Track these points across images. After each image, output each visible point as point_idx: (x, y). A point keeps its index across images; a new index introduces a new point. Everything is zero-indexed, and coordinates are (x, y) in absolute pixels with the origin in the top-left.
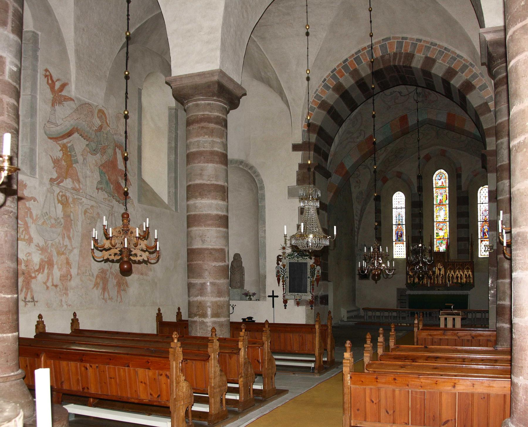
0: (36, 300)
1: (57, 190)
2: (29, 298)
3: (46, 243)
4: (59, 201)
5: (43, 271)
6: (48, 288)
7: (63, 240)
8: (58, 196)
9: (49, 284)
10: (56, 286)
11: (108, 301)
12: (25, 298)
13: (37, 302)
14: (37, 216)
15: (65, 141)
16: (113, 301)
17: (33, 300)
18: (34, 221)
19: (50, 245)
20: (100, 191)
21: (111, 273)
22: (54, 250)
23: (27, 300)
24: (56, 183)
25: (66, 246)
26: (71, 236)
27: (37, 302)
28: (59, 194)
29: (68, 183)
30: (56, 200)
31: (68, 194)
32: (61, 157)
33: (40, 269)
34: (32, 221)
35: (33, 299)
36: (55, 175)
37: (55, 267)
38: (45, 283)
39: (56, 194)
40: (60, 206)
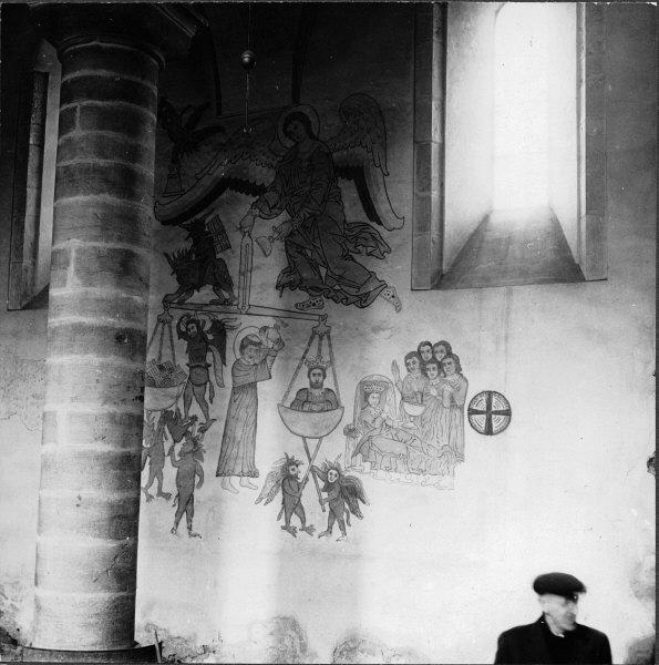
1: (177, 314)
4: (182, 335)
7: (187, 405)
10: (167, 496)
11: (299, 534)
15: (199, 216)
16: (316, 534)
19: (157, 419)
25: (195, 418)
26: (207, 396)
29: (204, 295)
30: (174, 331)
31: (201, 317)
37: (168, 459)
40: (182, 345)
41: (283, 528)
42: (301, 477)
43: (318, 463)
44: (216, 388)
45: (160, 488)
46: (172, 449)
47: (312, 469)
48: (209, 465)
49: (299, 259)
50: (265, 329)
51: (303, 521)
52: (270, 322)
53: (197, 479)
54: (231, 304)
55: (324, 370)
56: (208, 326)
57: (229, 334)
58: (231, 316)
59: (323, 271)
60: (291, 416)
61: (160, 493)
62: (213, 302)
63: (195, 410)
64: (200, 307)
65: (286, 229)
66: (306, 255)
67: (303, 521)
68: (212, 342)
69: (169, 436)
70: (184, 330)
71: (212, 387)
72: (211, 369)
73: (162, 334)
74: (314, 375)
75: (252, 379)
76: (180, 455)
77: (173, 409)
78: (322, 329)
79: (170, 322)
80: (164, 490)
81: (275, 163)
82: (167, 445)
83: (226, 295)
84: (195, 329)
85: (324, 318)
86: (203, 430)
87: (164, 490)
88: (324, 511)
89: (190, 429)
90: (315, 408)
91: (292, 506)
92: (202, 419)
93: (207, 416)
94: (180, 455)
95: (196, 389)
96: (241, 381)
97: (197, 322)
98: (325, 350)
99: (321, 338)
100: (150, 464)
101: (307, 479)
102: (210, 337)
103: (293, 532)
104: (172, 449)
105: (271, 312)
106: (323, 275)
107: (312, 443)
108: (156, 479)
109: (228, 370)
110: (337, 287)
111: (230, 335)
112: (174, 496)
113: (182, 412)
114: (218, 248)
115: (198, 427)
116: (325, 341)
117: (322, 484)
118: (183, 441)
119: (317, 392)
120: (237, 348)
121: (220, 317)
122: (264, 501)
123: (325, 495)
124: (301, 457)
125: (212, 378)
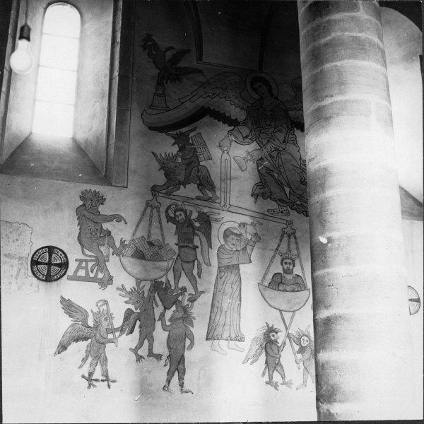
0: (111, 377)
1: (166, 202)
2: (98, 374)
3: (138, 284)
4: (170, 219)
5: (131, 332)
6: (139, 358)
7: (177, 278)
8: (167, 212)
9: (143, 351)
10: (159, 357)
11: (280, 387)
12: (91, 374)
13: (114, 381)
14: (122, 242)
15: (184, 130)
16: (294, 387)
17: (106, 379)
18: (118, 253)
20: (260, 198)
21: (288, 336)
22: (156, 295)
23: (94, 377)
24: (164, 192)
25: (184, 289)
26: (195, 272)
27: (114, 381)
28: (169, 207)
30: (163, 216)
31: (188, 208)
32: (175, 153)
33: (122, 326)
34: (111, 250)
35: (107, 377)
36: (161, 179)
37: (158, 324)
38: (135, 351)
39: (162, 209)
41: (267, 383)
42: (280, 341)
43: (293, 331)
44: (204, 266)
45: (150, 349)
46: (162, 316)
47: (288, 336)
48: (199, 330)
49: (269, 178)
50: (243, 225)
51: (283, 377)
52: (248, 220)
53: (188, 342)
54: (213, 202)
55: (293, 261)
56: (195, 216)
57: (213, 224)
58: (214, 210)
59: (287, 190)
60: (270, 293)
61: (151, 354)
62: (198, 198)
63: (184, 282)
64: (187, 199)
65: (257, 155)
66: (273, 176)
67: (283, 377)
68: (199, 229)
69: (160, 303)
70: (173, 216)
71: (199, 265)
72: (198, 250)
73: (151, 216)
74: (286, 263)
75: (235, 262)
76: (170, 320)
77: (164, 280)
78: (289, 230)
79: (158, 208)
80: (155, 351)
81: (245, 107)
82: (158, 311)
83: (210, 194)
84: (183, 216)
85: (290, 223)
86: (192, 300)
87: (155, 351)
88: (299, 369)
89: (180, 298)
90: (288, 288)
91: (273, 364)
92: (191, 290)
93: (196, 288)
94: (170, 320)
95: (186, 266)
96: (225, 262)
97: (185, 212)
98: (293, 246)
99: (289, 236)
100: (140, 327)
101: (284, 343)
102: (197, 224)
103: (276, 386)
104: (162, 316)
105: (247, 212)
106: (287, 192)
107: (287, 316)
108: (146, 341)
109: (214, 252)
110: (298, 202)
111: (215, 226)
112: (164, 358)
113: (172, 283)
114: (201, 158)
115: (187, 297)
116: (292, 240)
117: (297, 348)
118: (174, 308)
119: (289, 277)
120: (221, 236)
121: (205, 210)
122: (250, 361)
123: (299, 356)
124: (279, 325)
125: (200, 257)
